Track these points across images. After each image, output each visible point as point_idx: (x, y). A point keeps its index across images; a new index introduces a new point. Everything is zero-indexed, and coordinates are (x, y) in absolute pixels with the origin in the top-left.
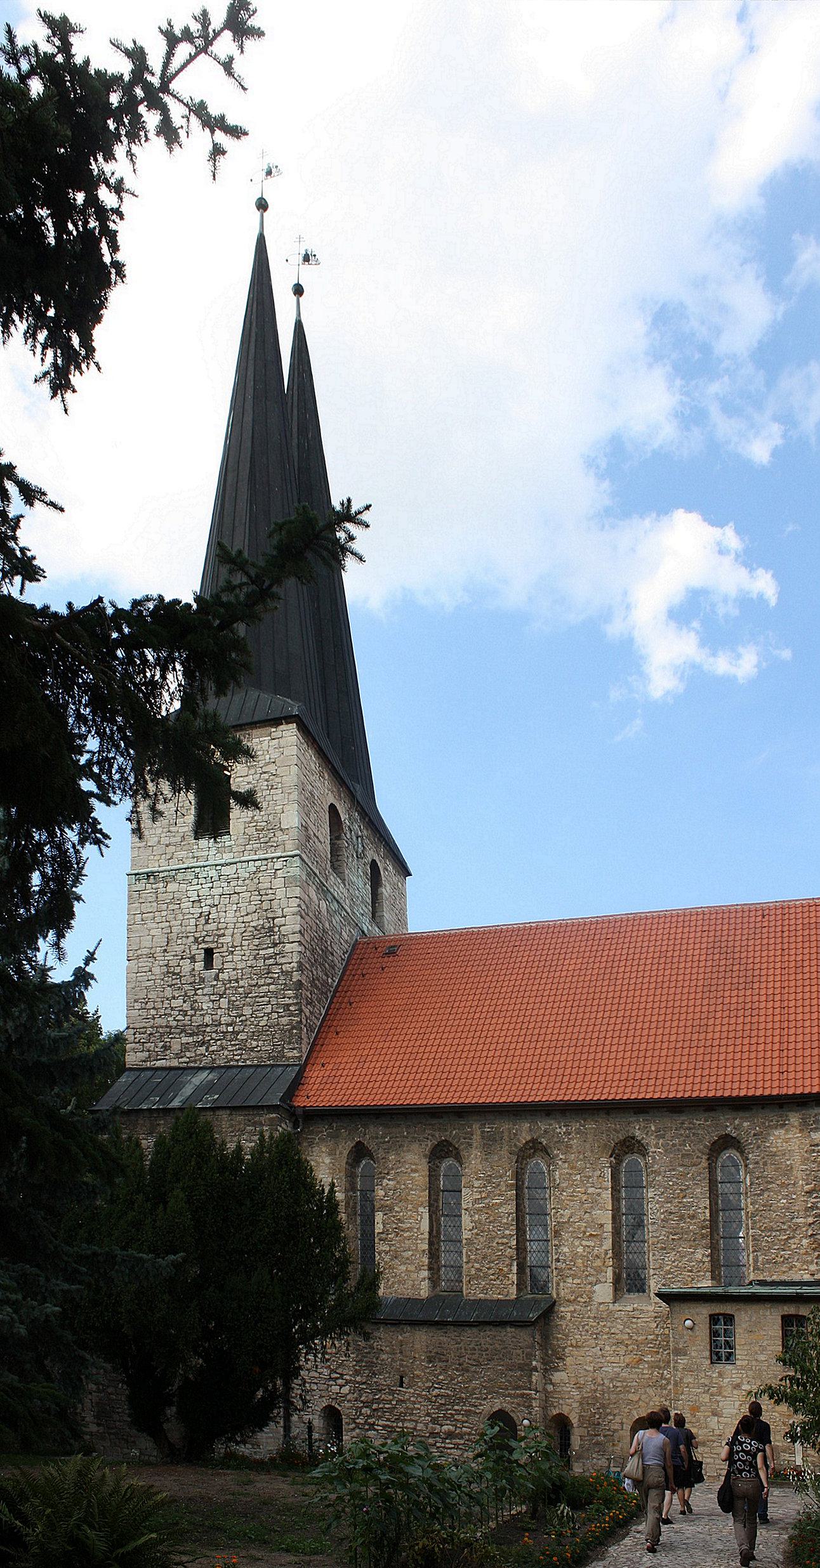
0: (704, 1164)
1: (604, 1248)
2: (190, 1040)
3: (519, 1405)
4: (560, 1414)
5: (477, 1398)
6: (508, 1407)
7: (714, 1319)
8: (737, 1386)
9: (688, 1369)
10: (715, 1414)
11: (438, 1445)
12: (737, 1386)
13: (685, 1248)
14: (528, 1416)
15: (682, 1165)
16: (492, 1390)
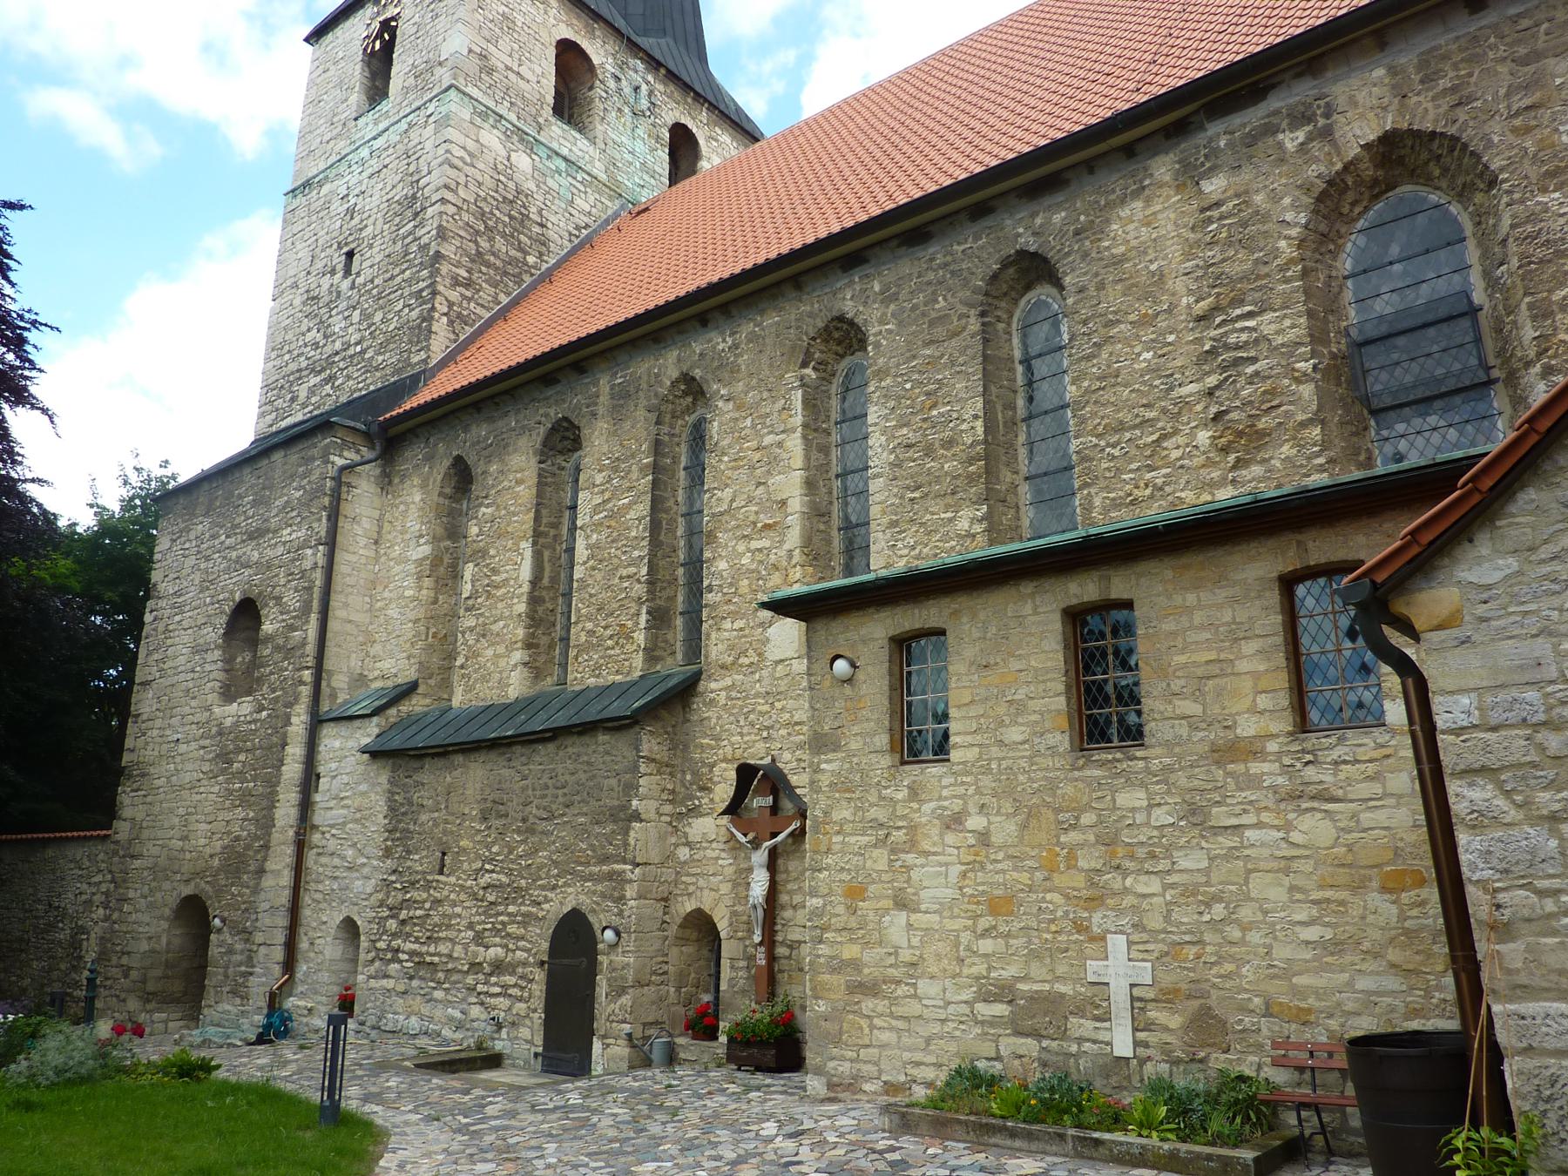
0: (974, 325)
1: (786, 546)
2: (318, 379)
3: (603, 896)
4: (699, 911)
5: (543, 888)
7: (903, 645)
9: (842, 786)
10: (902, 903)
11: (480, 988)
12: (954, 822)
13: (937, 512)
14: (615, 921)
15: (932, 342)
16: (566, 871)
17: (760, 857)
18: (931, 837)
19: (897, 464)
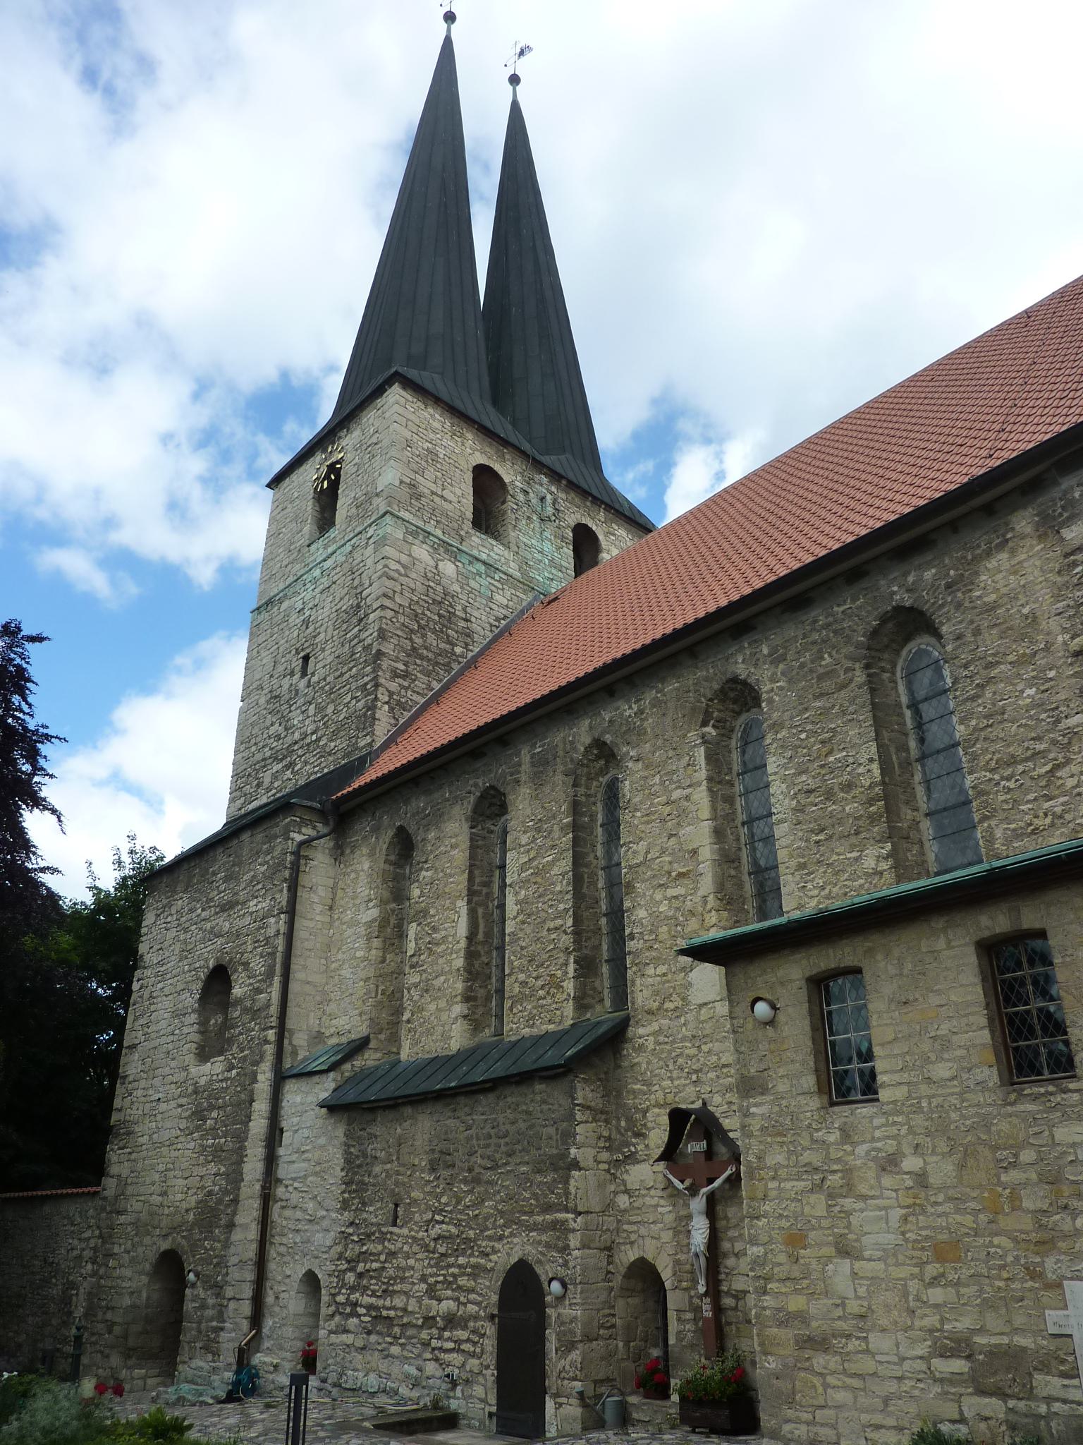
0: (860, 677)
1: (701, 893)
2: (280, 766)
3: (548, 1245)
5: (490, 1238)
6: (532, 1253)
7: (820, 985)
8: (890, 1163)
9: (774, 1130)
10: (844, 1250)
11: (434, 1343)
13: (842, 853)
14: (561, 1272)
15: (822, 695)
17: (698, 1204)
18: (867, 1180)
19: (800, 809)
